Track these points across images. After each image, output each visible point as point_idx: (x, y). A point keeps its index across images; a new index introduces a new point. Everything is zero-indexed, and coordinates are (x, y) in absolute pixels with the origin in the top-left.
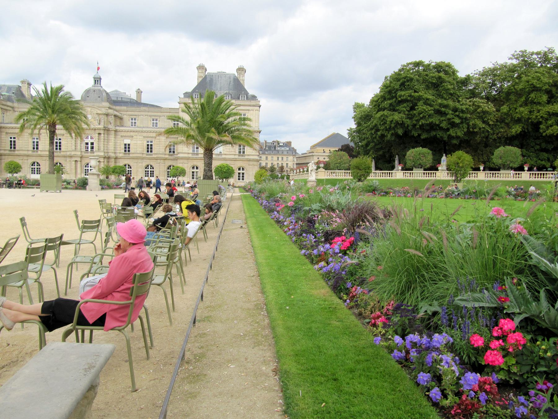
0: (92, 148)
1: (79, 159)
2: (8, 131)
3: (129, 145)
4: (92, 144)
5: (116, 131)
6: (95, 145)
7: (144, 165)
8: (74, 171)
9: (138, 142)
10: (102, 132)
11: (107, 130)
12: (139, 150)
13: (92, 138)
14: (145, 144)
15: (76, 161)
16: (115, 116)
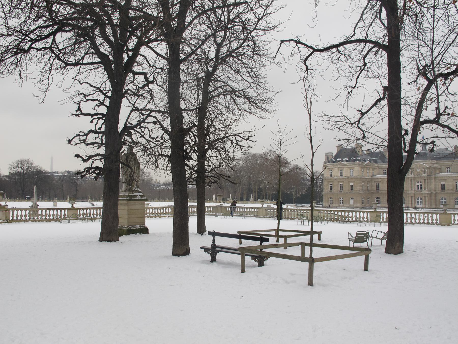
0: (421, 188)
1: (413, 195)
2: (375, 180)
3: (444, 185)
4: (421, 185)
5: (435, 177)
6: (423, 186)
7: (454, 197)
8: (410, 202)
9: (450, 183)
10: (426, 179)
11: (429, 178)
12: (451, 188)
13: (420, 182)
14: (455, 184)
15: (412, 197)
16: (434, 168)
